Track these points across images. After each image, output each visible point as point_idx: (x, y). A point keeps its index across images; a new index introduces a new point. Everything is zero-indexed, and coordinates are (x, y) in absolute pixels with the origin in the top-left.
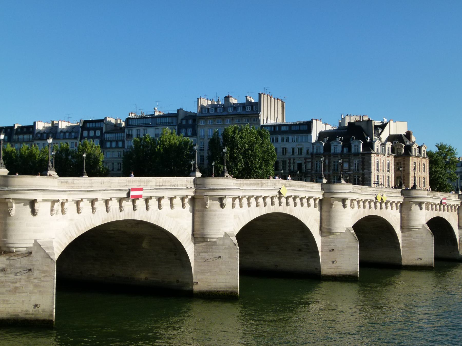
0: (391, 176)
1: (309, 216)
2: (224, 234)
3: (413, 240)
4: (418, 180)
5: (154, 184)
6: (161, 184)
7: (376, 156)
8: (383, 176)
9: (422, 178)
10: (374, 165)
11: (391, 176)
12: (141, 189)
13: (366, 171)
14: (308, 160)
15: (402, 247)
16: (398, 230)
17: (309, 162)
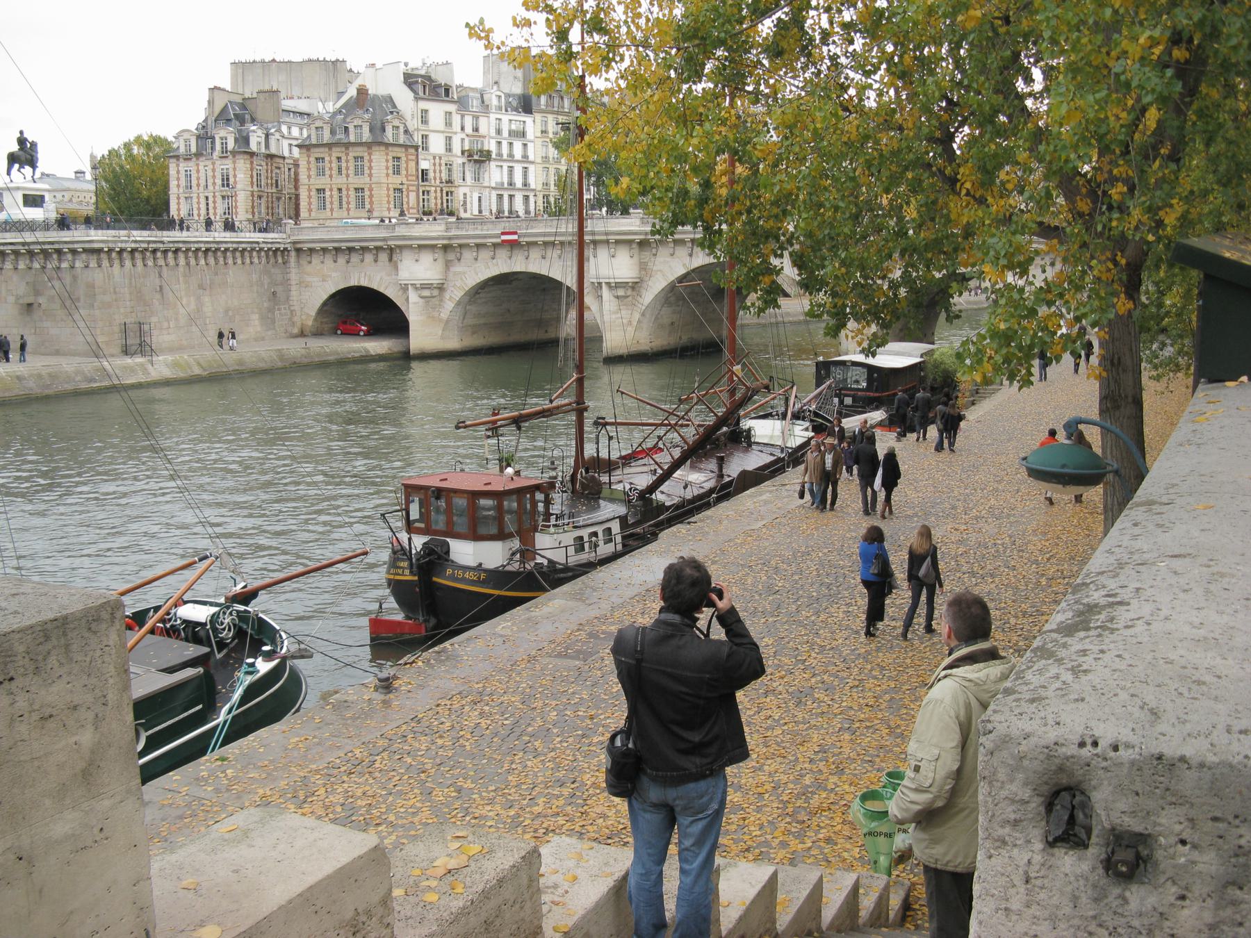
4: (331, 196)
9: (348, 189)
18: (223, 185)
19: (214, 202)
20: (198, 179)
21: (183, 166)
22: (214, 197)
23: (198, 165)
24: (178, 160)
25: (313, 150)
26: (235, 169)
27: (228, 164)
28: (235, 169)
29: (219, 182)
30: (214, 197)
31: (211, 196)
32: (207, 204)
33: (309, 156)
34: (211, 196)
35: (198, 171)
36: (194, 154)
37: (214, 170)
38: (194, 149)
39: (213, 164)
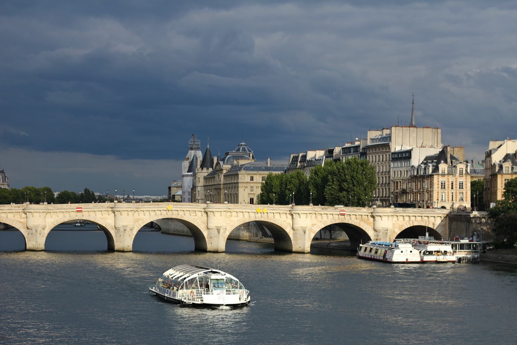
0: (466, 192)
1: (197, 220)
2: (121, 226)
3: (297, 236)
5: (92, 206)
6: (96, 206)
7: (440, 176)
8: (452, 193)
10: (438, 184)
11: (466, 192)
12: (81, 208)
13: (432, 189)
14: (410, 181)
15: (293, 240)
16: (288, 230)
17: (410, 182)
18: (460, 188)
19: (456, 195)
20: (448, 185)
21: (441, 179)
22: (456, 193)
23: (448, 179)
24: (438, 176)
25: (504, 176)
26: (466, 182)
27: (462, 179)
28: (466, 182)
29: (458, 186)
30: (456, 193)
31: (454, 192)
32: (452, 196)
33: (502, 178)
34: (454, 192)
35: (448, 182)
36: (446, 175)
37: (456, 182)
38: (446, 172)
39: (456, 179)
